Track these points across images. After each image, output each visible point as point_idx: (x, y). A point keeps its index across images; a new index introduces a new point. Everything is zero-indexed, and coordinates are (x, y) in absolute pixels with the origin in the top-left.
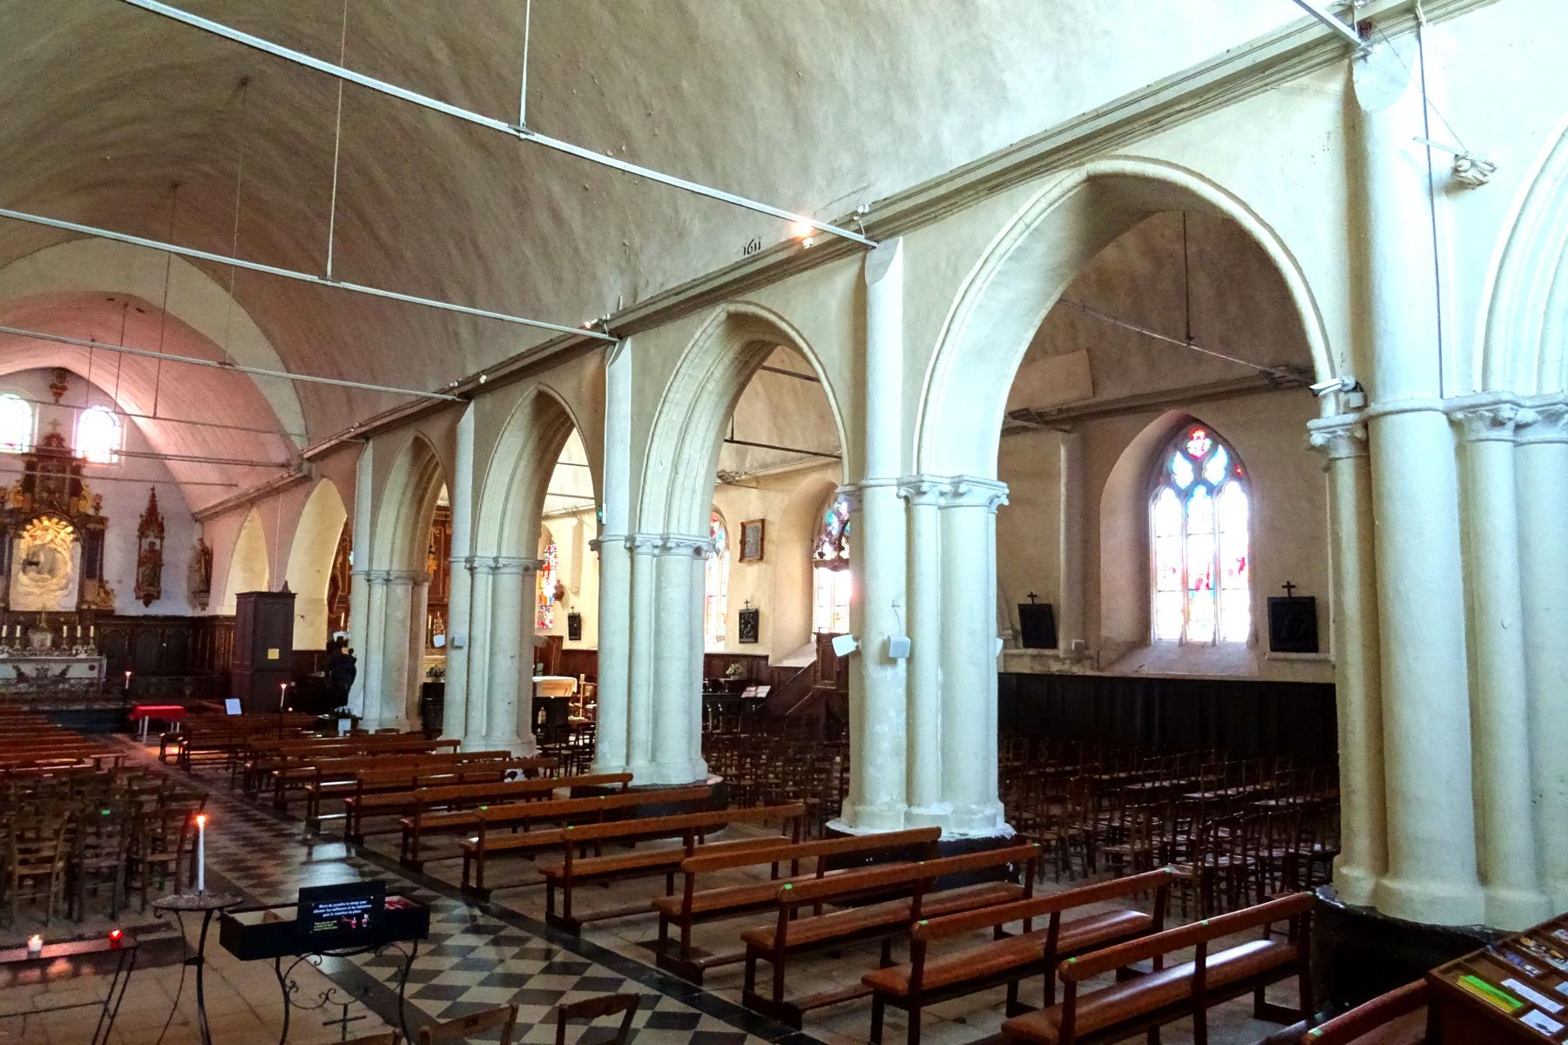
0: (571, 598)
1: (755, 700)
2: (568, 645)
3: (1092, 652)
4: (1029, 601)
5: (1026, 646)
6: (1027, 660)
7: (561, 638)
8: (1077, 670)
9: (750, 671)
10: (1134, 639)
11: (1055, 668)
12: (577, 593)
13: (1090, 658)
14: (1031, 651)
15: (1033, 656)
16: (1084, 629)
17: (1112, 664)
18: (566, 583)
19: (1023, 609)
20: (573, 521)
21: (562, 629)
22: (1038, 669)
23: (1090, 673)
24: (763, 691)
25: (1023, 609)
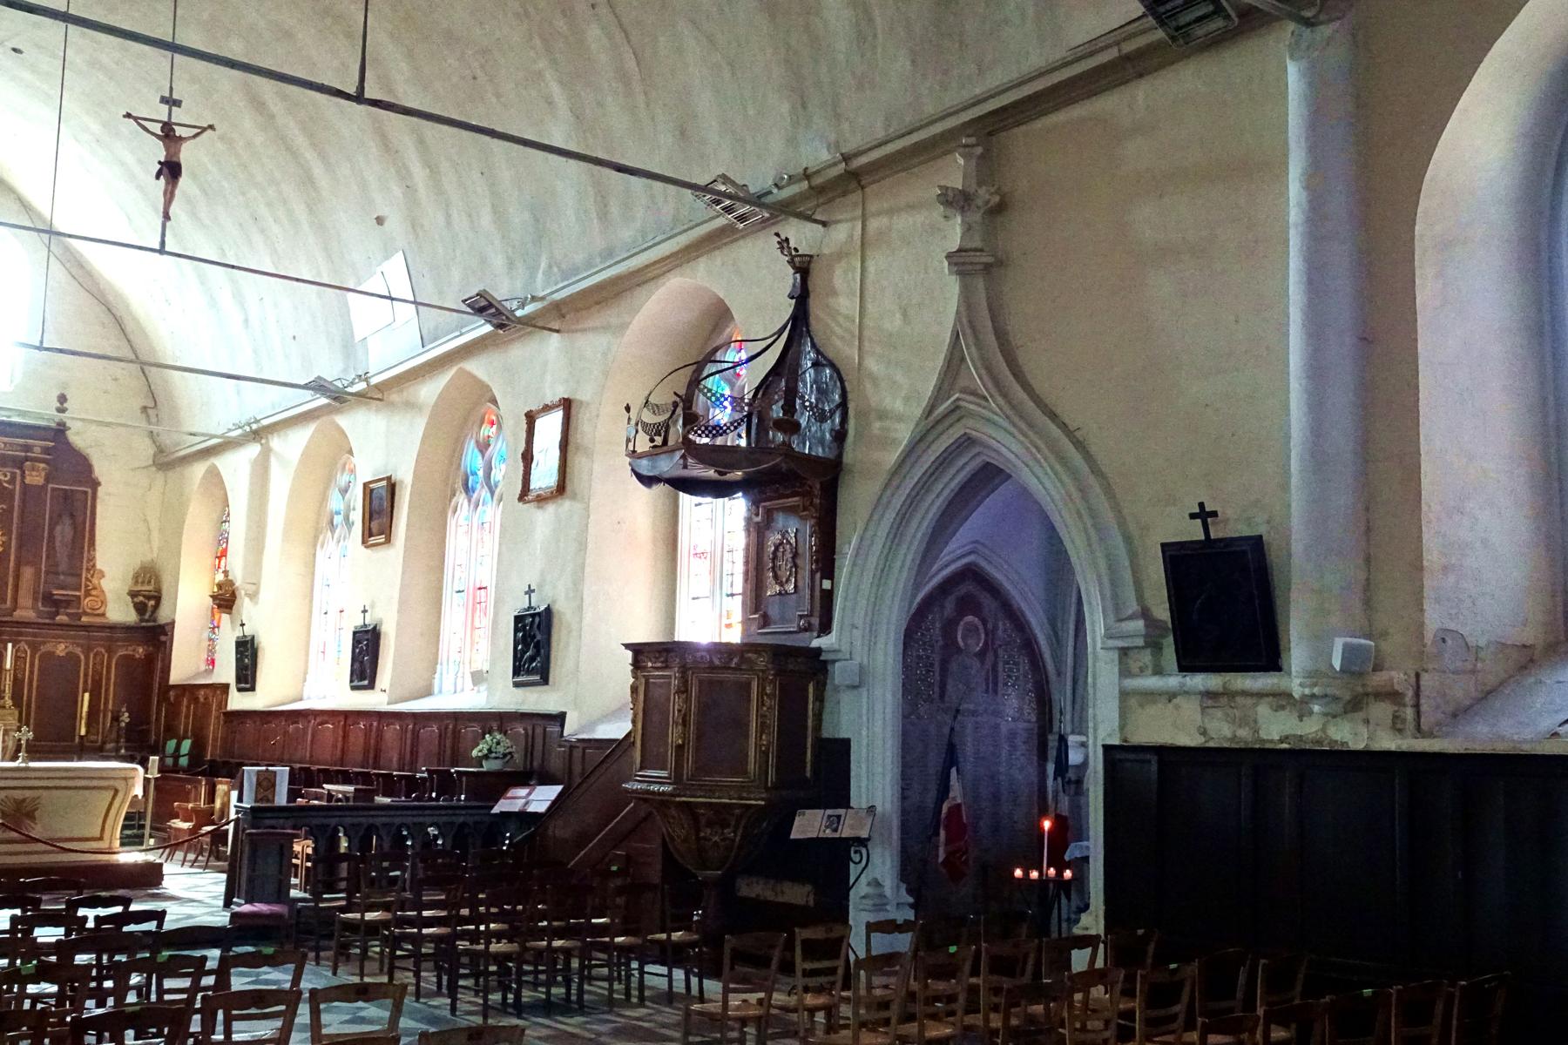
0: (245, 606)
1: (524, 818)
2: (238, 701)
3: (1397, 677)
4: (1195, 532)
5: (1185, 667)
6: (1190, 709)
7: (225, 688)
8: (1350, 735)
9: (529, 751)
10: (1530, 635)
11: (1276, 728)
12: (253, 596)
13: (1394, 696)
14: (1199, 681)
15: (1209, 695)
16: (1368, 603)
17: (1459, 714)
18: (238, 576)
19: (1178, 558)
20: (253, 450)
21: (226, 672)
22: (1222, 731)
23: (1388, 742)
24: (541, 798)
25: (1178, 558)
